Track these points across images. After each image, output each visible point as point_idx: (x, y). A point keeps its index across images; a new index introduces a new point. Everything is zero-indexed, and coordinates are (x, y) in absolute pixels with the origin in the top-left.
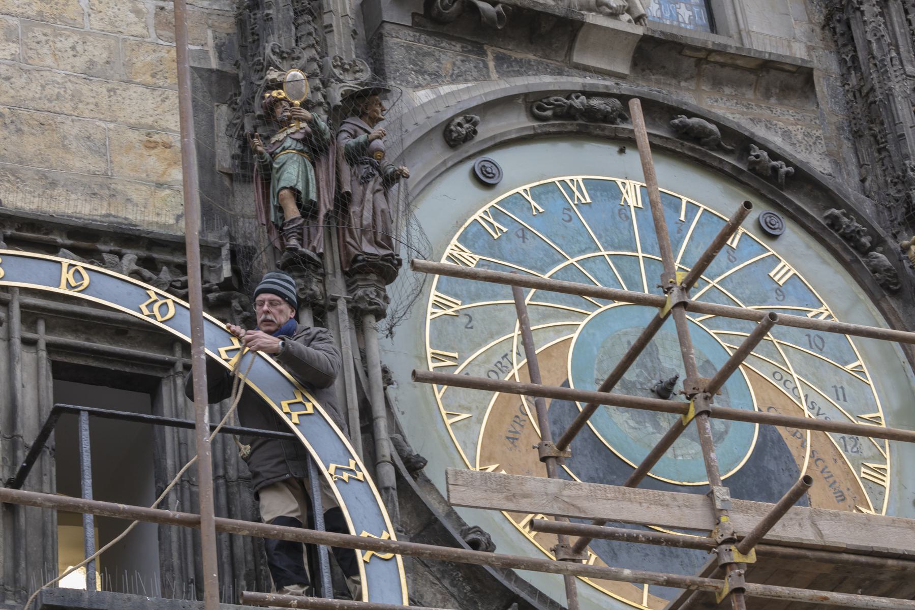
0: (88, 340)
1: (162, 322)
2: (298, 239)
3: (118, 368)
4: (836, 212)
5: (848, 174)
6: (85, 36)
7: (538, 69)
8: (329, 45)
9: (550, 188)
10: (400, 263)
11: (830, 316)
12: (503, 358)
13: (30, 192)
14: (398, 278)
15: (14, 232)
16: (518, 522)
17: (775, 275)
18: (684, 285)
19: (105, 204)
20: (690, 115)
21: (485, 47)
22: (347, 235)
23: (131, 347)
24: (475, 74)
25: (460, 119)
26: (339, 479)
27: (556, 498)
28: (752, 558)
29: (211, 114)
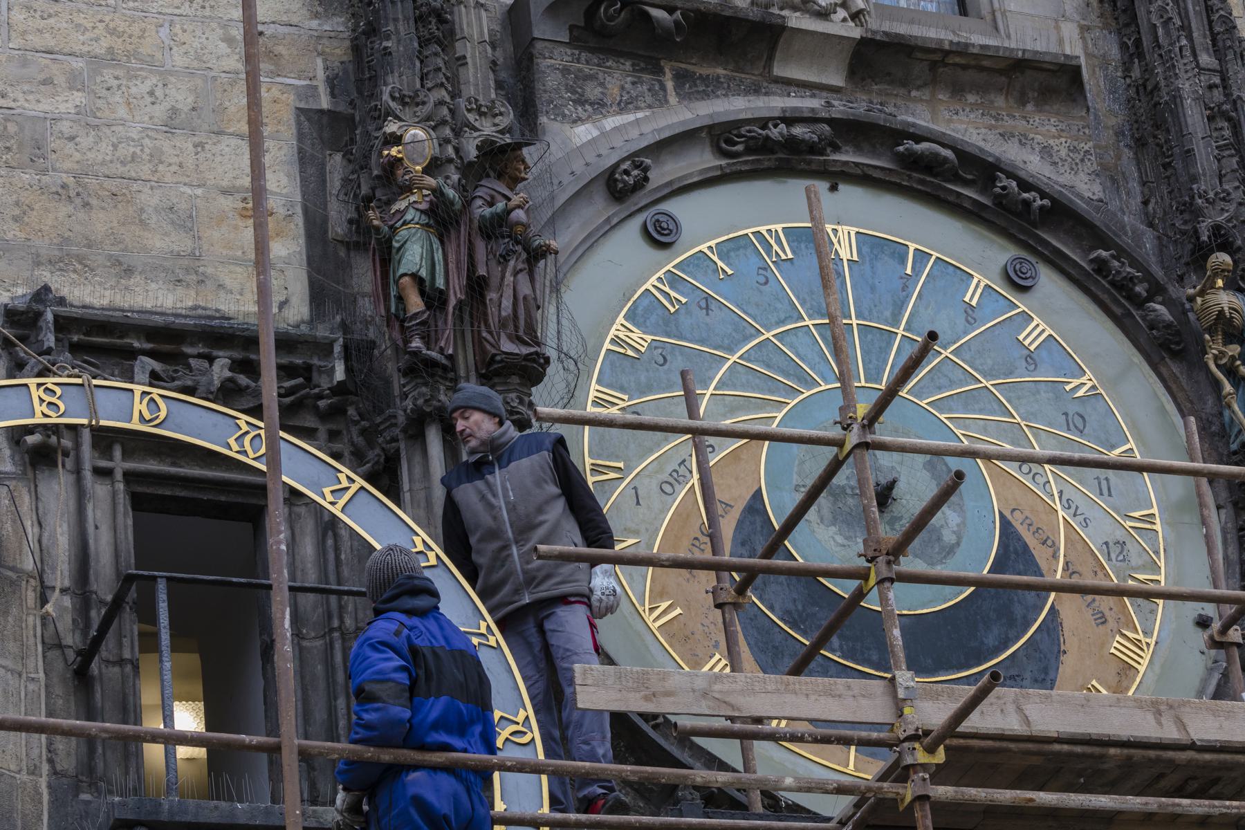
0: (174, 464)
2: (422, 338)
3: (211, 497)
4: (1104, 254)
5: (1128, 194)
6: (165, 75)
9: (742, 242)
10: (547, 361)
11: (1094, 387)
13: (100, 284)
14: (546, 379)
15: (82, 337)
17: (1025, 339)
18: (865, 422)
19: (193, 293)
20: (918, 139)
22: (483, 328)
23: (226, 471)
24: (649, 99)
25: (625, 166)
27: (705, 694)
28: (940, 756)
29: (323, 165)
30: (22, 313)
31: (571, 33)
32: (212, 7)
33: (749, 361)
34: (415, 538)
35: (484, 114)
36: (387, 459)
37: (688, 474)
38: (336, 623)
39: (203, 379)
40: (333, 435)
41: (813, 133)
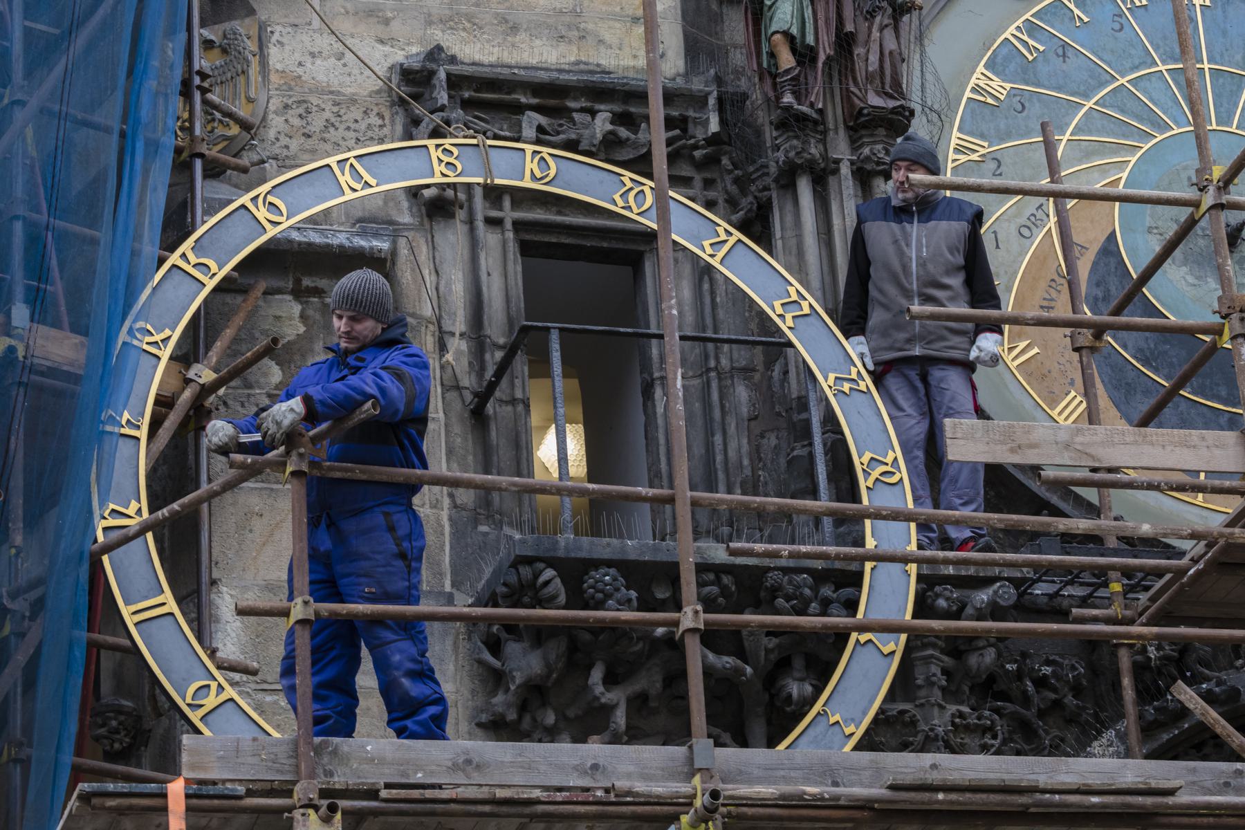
0: (559, 213)
2: (793, 93)
10: (912, 113)
13: (488, 41)
15: (473, 94)
16: (1052, 409)
18: (1221, 184)
19: (575, 49)
27: (1067, 446)
30: (417, 72)
33: (1104, 106)
34: (789, 288)
36: (760, 207)
37: (1045, 218)
38: (712, 364)
39: (586, 132)
40: (708, 184)
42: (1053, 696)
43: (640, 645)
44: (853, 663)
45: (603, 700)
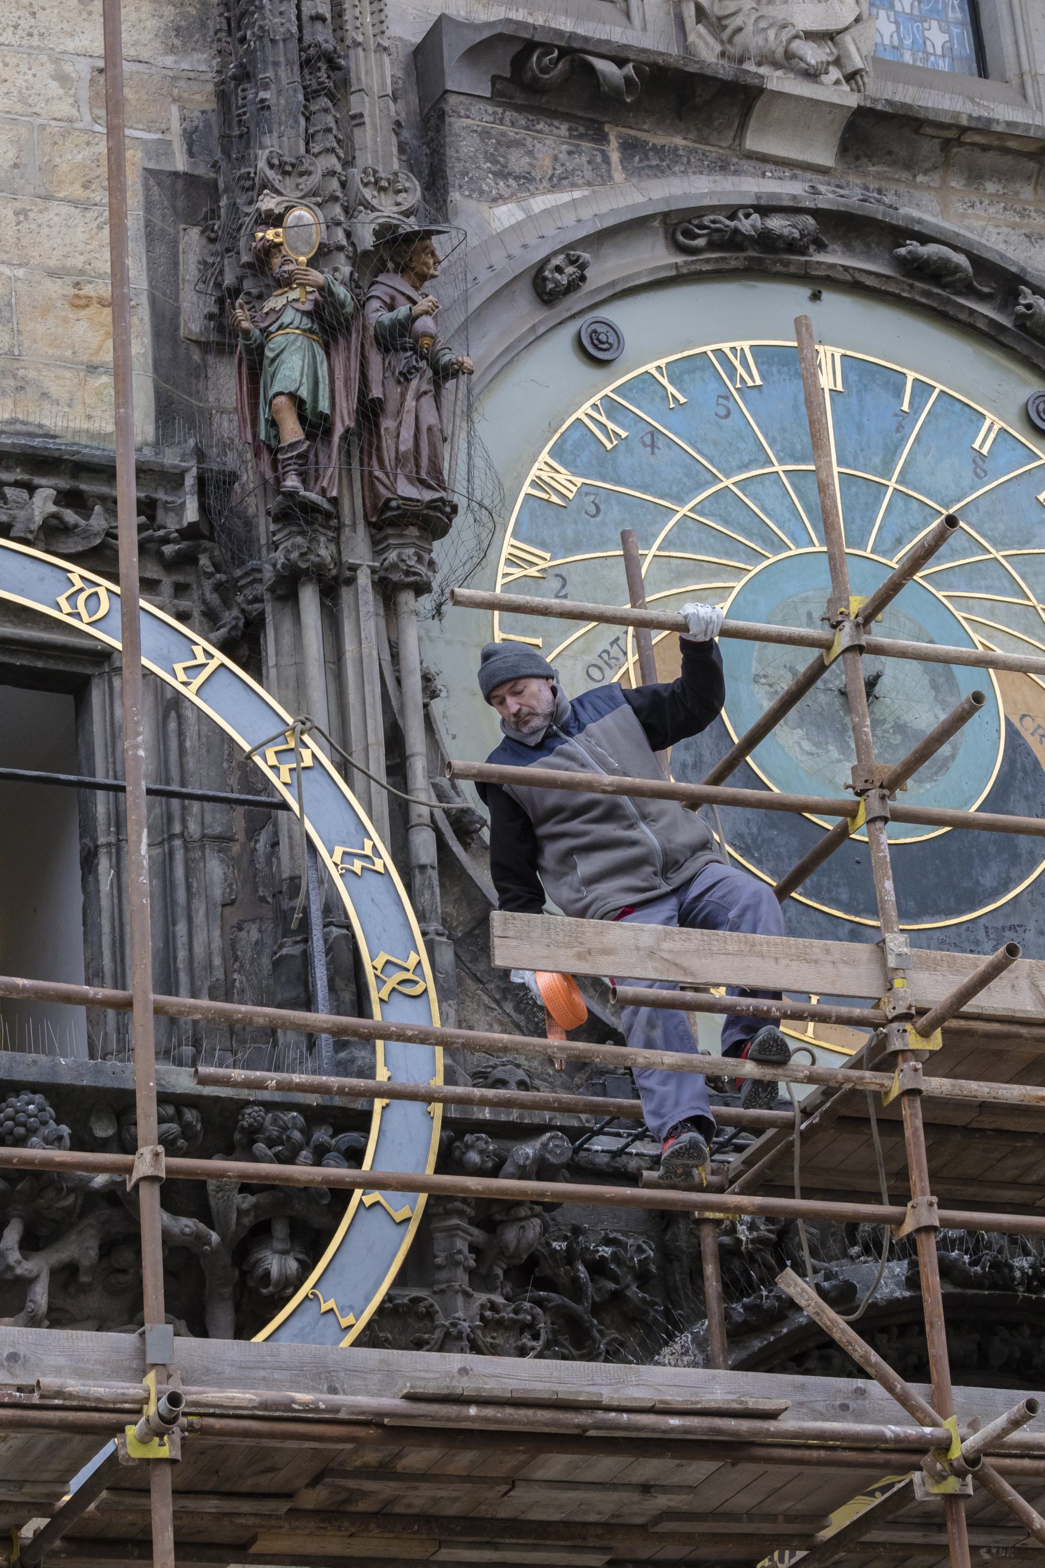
1: (89, 624)
2: (300, 474)
3: (25, 662)
7: (689, 161)
8: (357, 146)
9: (699, 363)
10: (455, 509)
12: (612, 644)
18: (860, 620)
19: (9, 403)
20: (924, 239)
21: (607, 128)
24: (588, 174)
25: (559, 260)
26: (347, 870)
27: (652, 954)
28: (936, 1042)
29: (174, 243)
31: (493, 85)
32: (41, 35)
35: (383, 189)
36: (248, 624)
37: (621, 656)
38: (177, 828)
39: (21, 514)
40: (180, 589)
41: (794, 226)
42: (612, 1286)
43: (70, 1200)
44: (354, 1232)
45: (19, 1271)
